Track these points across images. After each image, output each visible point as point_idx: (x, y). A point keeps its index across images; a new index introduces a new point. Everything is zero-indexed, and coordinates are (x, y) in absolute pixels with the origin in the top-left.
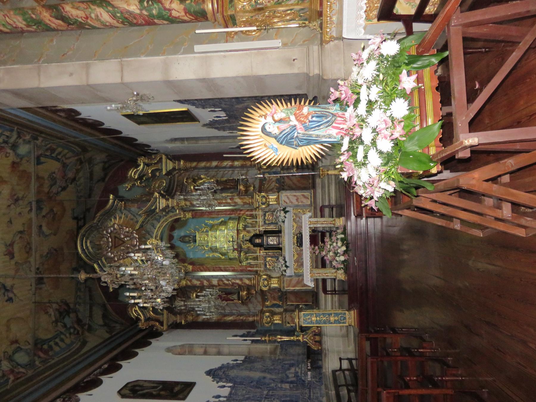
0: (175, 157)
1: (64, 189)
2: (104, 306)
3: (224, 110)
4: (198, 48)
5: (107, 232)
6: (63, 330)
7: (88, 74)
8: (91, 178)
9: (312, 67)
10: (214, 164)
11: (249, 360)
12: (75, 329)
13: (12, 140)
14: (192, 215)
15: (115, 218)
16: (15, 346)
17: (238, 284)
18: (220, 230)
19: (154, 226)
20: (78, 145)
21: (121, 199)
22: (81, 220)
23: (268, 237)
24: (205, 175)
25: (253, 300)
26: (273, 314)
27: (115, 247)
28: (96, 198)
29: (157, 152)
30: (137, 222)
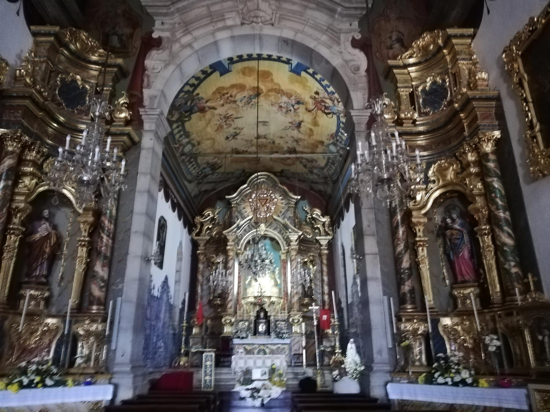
0: (331, 245)
1: (305, 166)
2: (214, 189)
4: (385, 297)
5: (271, 194)
6: (201, 168)
7: (370, 235)
8: (313, 182)
9: (377, 365)
10: (326, 278)
11: (171, 307)
12: (201, 175)
13: (338, 143)
14: (283, 260)
15: (282, 200)
16: (196, 143)
17: (228, 298)
19: (275, 229)
20: (338, 178)
21: (296, 204)
22: (281, 174)
23: (265, 323)
25: (212, 310)
26: (201, 326)
27: (259, 200)
28: (297, 184)
29: (334, 232)
30: (279, 216)
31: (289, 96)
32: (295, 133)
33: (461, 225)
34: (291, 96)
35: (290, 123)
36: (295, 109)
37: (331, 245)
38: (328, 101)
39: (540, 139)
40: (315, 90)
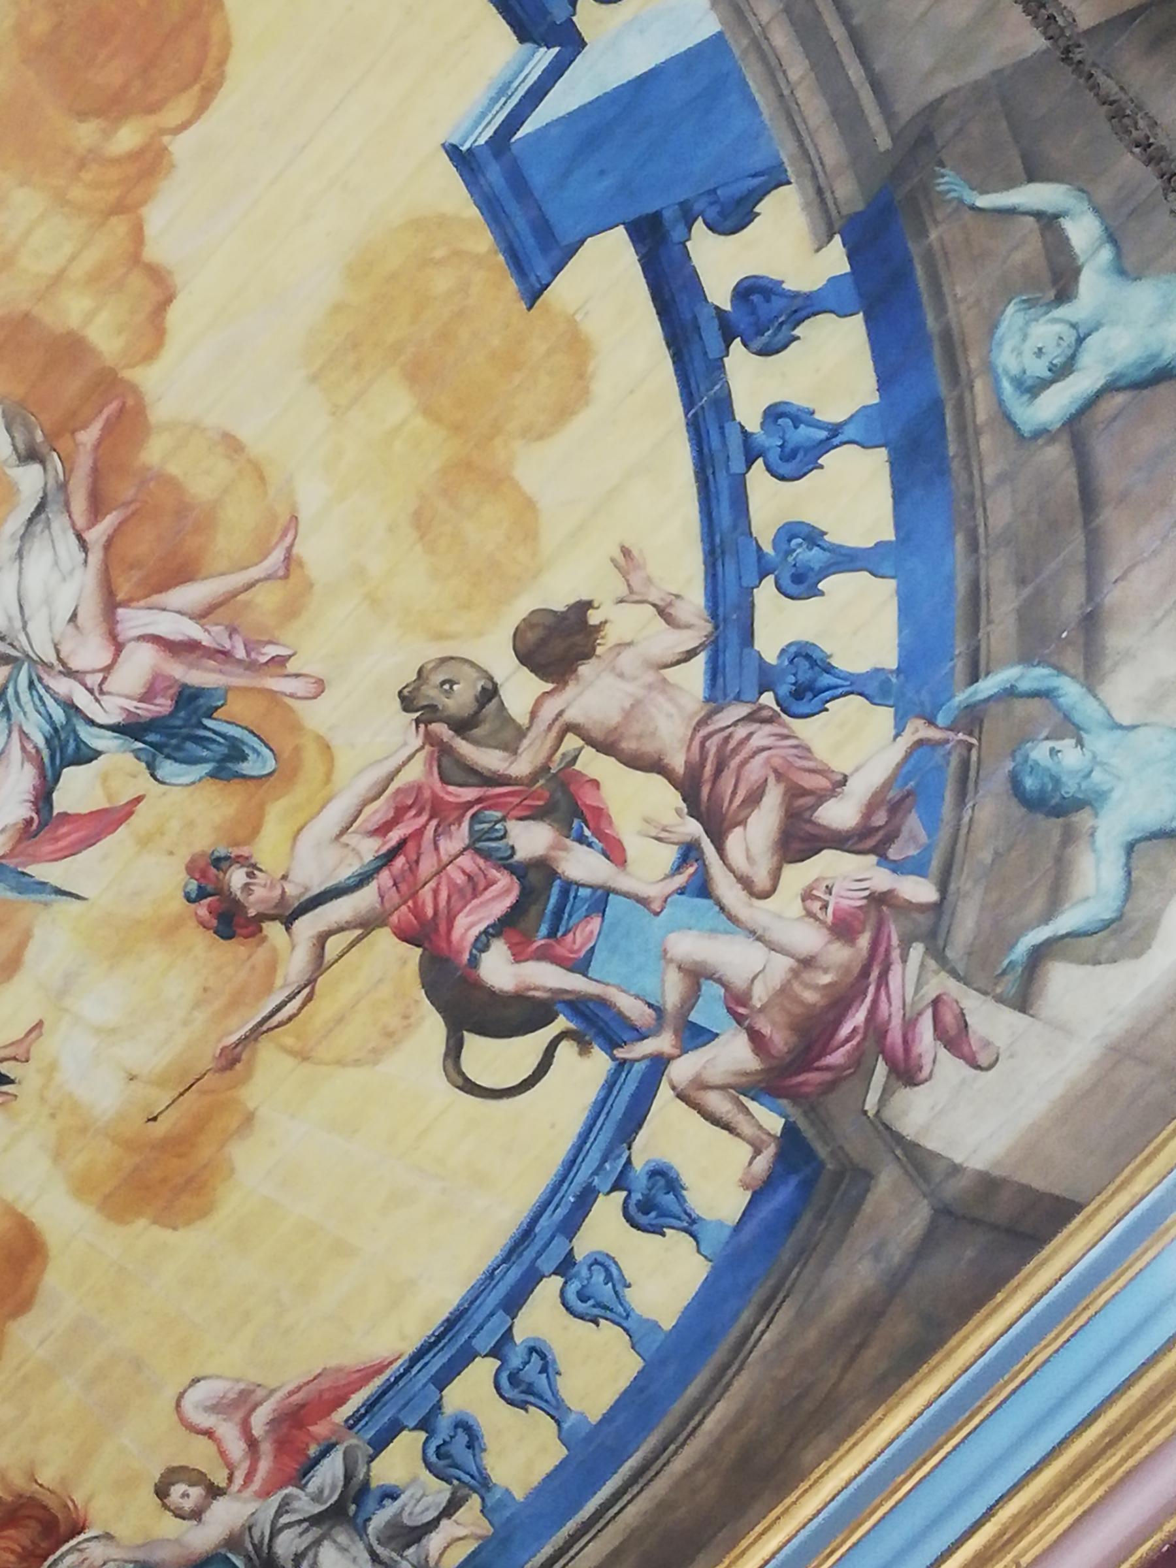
34: (178, 571)
38: (642, 807)
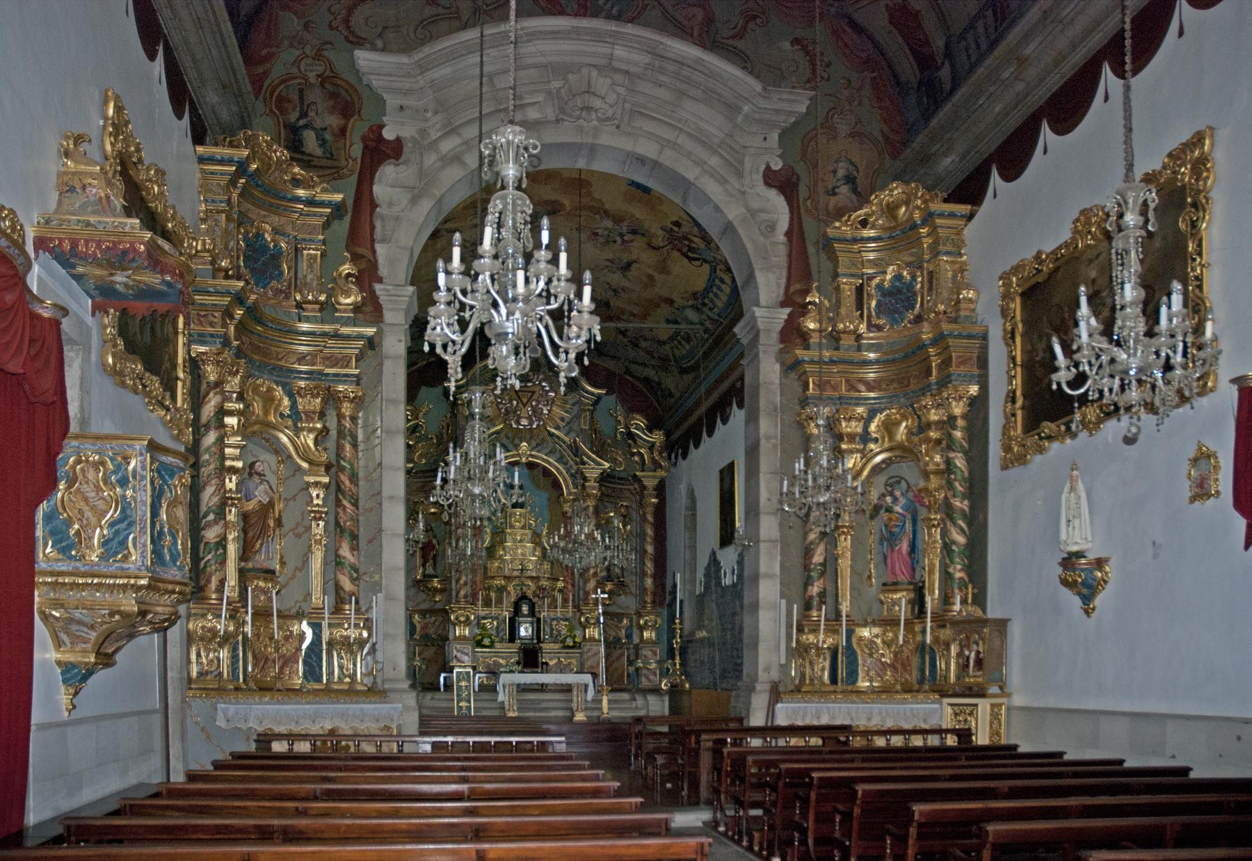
3: (734, 585)
7: (768, 513)
18: (535, 549)
21: (596, 403)
24: (631, 532)
31: (618, 220)
32: (616, 278)
33: (906, 508)
35: (612, 261)
36: (624, 242)
37: (661, 489)
39: (1019, 418)
40: (674, 219)
